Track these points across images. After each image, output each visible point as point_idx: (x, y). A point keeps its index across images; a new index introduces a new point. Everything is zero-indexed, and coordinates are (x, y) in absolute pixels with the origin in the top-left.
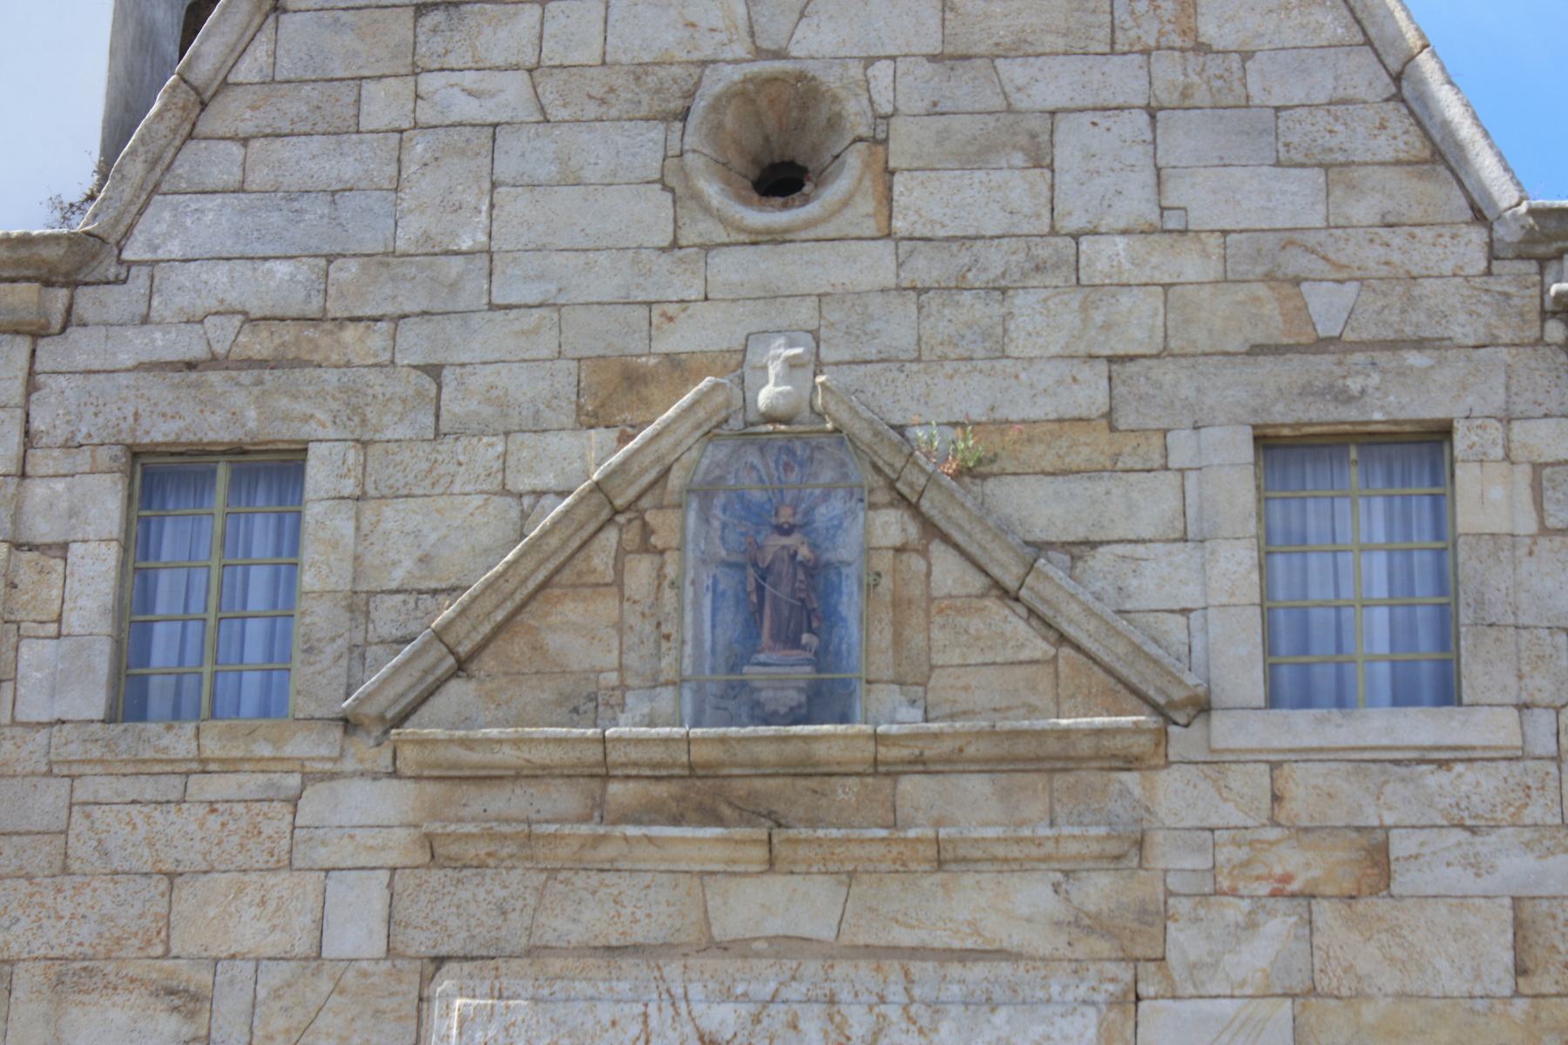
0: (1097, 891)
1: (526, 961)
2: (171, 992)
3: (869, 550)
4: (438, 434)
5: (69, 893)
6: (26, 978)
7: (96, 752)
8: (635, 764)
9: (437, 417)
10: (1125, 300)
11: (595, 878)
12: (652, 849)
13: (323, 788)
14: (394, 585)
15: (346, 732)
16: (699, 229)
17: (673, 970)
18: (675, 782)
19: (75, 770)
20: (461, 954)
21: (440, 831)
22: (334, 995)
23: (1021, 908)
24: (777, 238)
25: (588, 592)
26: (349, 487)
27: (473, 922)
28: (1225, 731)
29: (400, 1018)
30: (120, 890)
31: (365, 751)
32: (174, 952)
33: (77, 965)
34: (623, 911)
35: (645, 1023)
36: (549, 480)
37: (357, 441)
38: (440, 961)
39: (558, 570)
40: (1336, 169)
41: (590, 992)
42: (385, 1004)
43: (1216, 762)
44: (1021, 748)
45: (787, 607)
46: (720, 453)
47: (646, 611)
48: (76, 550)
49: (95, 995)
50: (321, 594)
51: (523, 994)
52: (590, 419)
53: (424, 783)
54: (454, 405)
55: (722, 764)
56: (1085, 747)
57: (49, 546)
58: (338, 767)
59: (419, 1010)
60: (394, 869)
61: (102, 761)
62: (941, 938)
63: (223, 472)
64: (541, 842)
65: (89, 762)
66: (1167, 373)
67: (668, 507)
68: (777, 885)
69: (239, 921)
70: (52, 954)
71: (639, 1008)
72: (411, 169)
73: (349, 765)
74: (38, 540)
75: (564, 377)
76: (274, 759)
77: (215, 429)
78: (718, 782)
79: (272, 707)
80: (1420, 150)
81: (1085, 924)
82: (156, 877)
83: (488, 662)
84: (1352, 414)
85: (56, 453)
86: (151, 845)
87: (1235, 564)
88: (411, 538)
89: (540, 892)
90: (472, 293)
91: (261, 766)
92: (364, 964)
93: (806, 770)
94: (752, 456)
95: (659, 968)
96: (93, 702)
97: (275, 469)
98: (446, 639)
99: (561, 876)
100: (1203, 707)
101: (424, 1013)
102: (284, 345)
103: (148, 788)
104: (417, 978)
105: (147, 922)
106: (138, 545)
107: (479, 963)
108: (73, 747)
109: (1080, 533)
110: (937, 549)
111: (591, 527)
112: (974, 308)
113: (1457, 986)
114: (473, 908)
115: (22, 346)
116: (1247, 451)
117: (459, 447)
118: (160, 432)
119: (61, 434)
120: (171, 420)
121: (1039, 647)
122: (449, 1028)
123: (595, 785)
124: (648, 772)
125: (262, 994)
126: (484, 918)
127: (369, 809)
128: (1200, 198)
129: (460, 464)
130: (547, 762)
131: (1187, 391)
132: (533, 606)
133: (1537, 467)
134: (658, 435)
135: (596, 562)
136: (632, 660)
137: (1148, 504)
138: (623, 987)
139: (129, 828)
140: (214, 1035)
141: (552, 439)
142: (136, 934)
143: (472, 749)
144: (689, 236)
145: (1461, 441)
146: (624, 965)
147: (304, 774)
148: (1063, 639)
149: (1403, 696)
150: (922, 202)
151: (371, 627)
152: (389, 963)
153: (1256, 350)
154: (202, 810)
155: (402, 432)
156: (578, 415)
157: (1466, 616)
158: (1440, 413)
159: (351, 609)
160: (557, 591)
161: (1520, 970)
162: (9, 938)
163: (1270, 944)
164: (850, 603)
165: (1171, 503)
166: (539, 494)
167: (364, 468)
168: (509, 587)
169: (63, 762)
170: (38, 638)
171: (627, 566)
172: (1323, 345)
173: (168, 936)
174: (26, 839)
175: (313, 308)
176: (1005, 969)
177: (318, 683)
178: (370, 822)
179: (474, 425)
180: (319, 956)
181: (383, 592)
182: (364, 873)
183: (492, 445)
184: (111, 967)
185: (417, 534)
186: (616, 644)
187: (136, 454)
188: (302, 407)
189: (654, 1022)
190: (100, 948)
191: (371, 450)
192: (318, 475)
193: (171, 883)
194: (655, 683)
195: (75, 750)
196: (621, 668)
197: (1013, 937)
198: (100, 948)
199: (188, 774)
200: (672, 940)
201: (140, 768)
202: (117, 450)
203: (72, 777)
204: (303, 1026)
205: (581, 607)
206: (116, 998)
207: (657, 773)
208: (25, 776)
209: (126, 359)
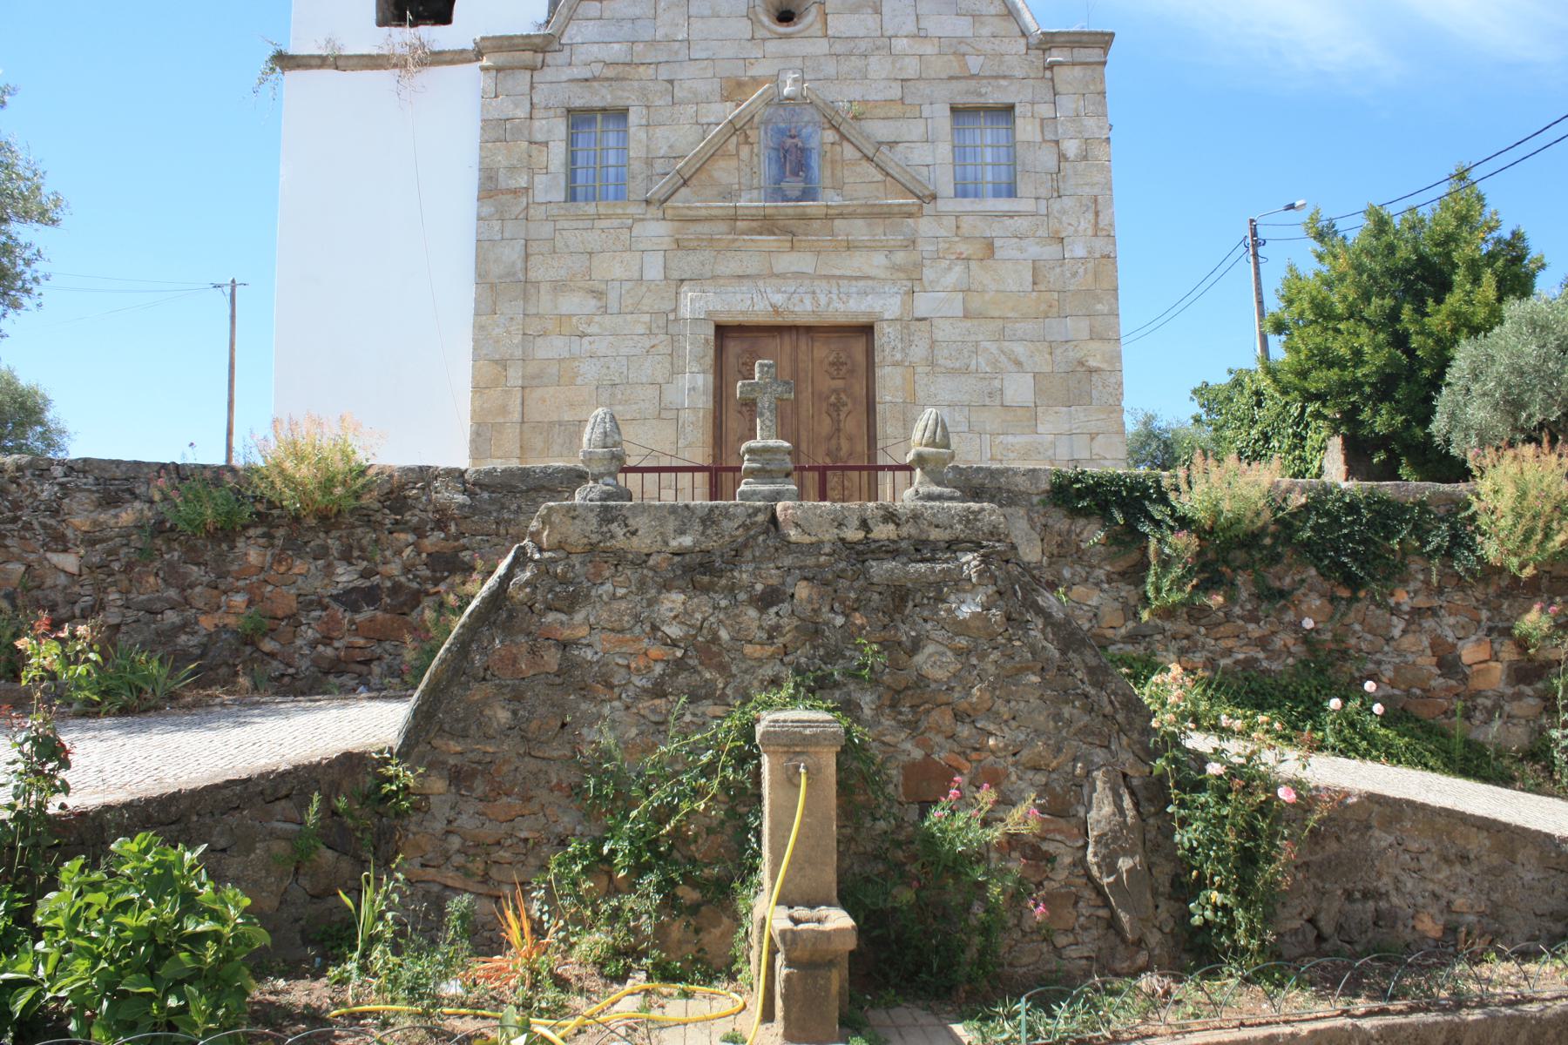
0: (900, 257)
3: (823, 144)
6: (544, 288)
10: (907, 60)
16: (761, 33)
17: (761, 283)
23: (876, 263)
24: (787, 36)
26: (644, 122)
28: (942, 205)
31: (654, 211)
36: (712, 119)
38: (682, 281)
40: (976, 17)
43: (938, 215)
44: (875, 210)
45: (793, 161)
46: (771, 110)
54: (678, 94)
56: (896, 210)
62: (849, 273)
63: (599, 117)
66: (921, 85)
68: (794, 255)
69: (614, 268)
72: (660, 11)
75: (716, 84)
77: (596, 102)
79: (620, 196)
80: (1001, 9)
81: (896, 268)
83: (694, 181)
84: (982, 100)
87: (944, 150)
90: (683, 55)
93: (804, 217)
94: (781, 112)
96: (559, 195)
97: (620, 114)
100: (934, 197)
102: (619, 71)
103: (581, 224)
106: (572, 141)
109: (892, 139)
110: (845, 144)
112: (856, 62)
113: (1015, 288)
115: (528, 73)
116: (948, 113)
118: (578, 103)
120: (582, 98)
121: (880, 177)
127: (656, 231)
128: (932, 26)
131: (928, 91)
133: (1042, 120)
137: (916, 130)
144: (757, 35)
145: (1018, 110)
148: (888, 174)
149: (997, 194)
150: (837, 25)
153: (951, 78)
155: (661, 103)
157: (1019, 168)
158: (1011, 101)
161: (1035, 283)
163: (955, 275)
164: (814, 162)
165: (923, 129)
172: (973, 77)
175: (628, 60)
176: (870, 283)
177: (637, 188)
187: (569, 111)
188: (626, 94)
192: (633, 117)
194: (751, 188)
195: (555, 212)
197: (873, 272)
201: (578, 218)
209: (564, 78)
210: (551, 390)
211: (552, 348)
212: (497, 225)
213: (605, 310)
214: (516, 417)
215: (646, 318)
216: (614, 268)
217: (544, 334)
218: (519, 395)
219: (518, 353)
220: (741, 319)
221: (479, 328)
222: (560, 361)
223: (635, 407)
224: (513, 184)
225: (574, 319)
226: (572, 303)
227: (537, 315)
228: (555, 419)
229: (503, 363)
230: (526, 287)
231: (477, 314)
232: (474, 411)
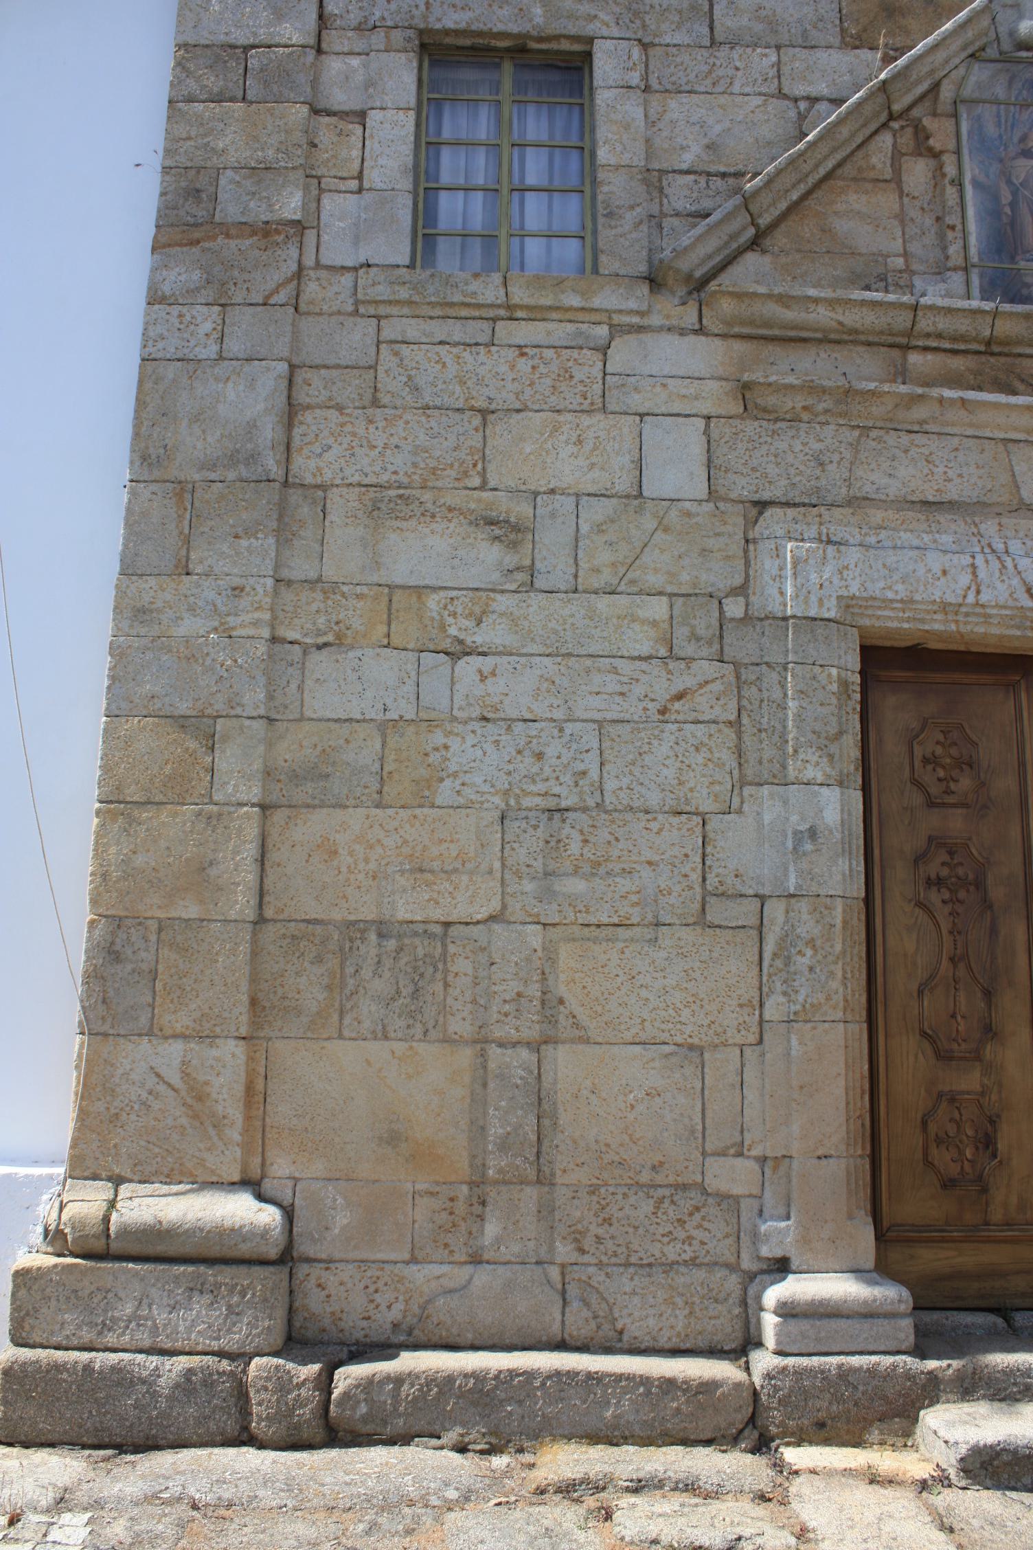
1: (848, 511)
2: (491, 522)
4: (713, 42)
5: (381, 424)
7: (404, 293)
8: (939, 336)
9: (712, 29)
11: (905, 439)
12: (963, 413)
13: (632, 339)
14: (684, 166)
15: (651, 290)
17: (989, 527)
18: (970, 357)
19: (382, 310)
20: (784, 500)
21: (762, 380)
22: (659, 532)
25: (869, 186)
27: (792, 471)
29: (728, 557)
30: (433, 424)
31: (671, 308)
32: (492, 484)
33: (392, 493)
34: (936, 470)
35: (974, 574)
36: (822, 89)
37: (640, 40)
38: (762, 505)
39: (839, 165)
41: (916, 542)
42: (711, 543)
47: (925, 206)
48: (374, 117)
49: (413, 522)
50: (617, 167)
51: (852, 541)
52: (856, 41)
53: (731, 341)
55: (1019, 342)
57: (347, 113)
58: (645, 322)
59: (746, 551)
60: (708, 418)
61: (410, 303)
64: (858, 399)
65: (398, 302)
67: (942, 115)
69: (555, 457)
70: (366, 481)
71: (967, 560)
73: (655, 320)
74: (336, 108)
76: (583, 309)
78: (1009, 360)
82: (468, 413)
83: (780, 239)
85: (350, 34)
86: (462, 383)
88: (697, 127)
89: (855, 447)
91: (569, 316)
92: (687, 504)
95: (976, 525)
96: (394, 247)
98: (751, 207)
99: (874, 433)
101: (752, 554)
103: (456, 331)
104: (741, 520)
105: (462, 455)
107: (802, 509)
108: (380, 288)
111: (873, 127)
114: (790, 459)
117: (735, 54)
119: (354, 17)
122: (782, 568)
123: (895, 353)
124: (947, 345)
125: (584, 528)
126: (802, 468)
127: (679, 362)
129: (737, 69)
130: (858, 326)
132: (819, 194)
134: (935, 47)
135: (874, 160)
136: (915, 248)
138: (947, 539)
139: (439, 367)
140: (538, 565)
141: (821, 55)
142: (452, 465)
143: (788, 307)
146: (942, 520)
147: (611, 326)
151: (665, 201)
152: (711, 505)
154: (512, 354)
155: (678, 38)
156: (843, 37)
159: (646, 182)
160: (840, 183)
162: (321, 464)
166: (813, 100)
167: (647, 66)
168: (806, 168)
169: (369, 302)
170: (340, 192)
171: (904, 167)
173: (484, 469)
174: (335, 373)
178: (681, 374)
179: (748, 38)
180: (641, 494)
181: (674, 171)
182: (681, 420)
183: (766, 55)
184: (427, 496)
185: (702, 124)
186: (900, 233)
189: (982, 574)
190: (416, 477)
191: (651, 52)
193: (484, 420)
195: (382, 291)
196: (905, 254)
198: (416, 477)
199: (494, 320)
200: (983, 499)
201: (448, 310)
202: (411, 33)
203: (378, 318)
204: (629, 561)
205: (864, 198)
206: (434, 526)
207: (956, 347)
208: (331, 315)
210: (355, 818)
211: (360, 686)
212: (206, 320)
213: (528, 579)
214: (242, 904)
215: (658, 608)
216: (555, 457)
217: (335, 642)
218: (252, 831)
219: (254, 698)
220: (938, 628)
221: (133, 613)
222: (386, 727)
223: (624, 884)
224: (259, 212)
225: (433, 602)
226: (427, 553)
227: (314, 583)
228: (368, 913)
229: (202, 728)
230: (287, 498)
231: (129, 569)
232: (102, 877)
